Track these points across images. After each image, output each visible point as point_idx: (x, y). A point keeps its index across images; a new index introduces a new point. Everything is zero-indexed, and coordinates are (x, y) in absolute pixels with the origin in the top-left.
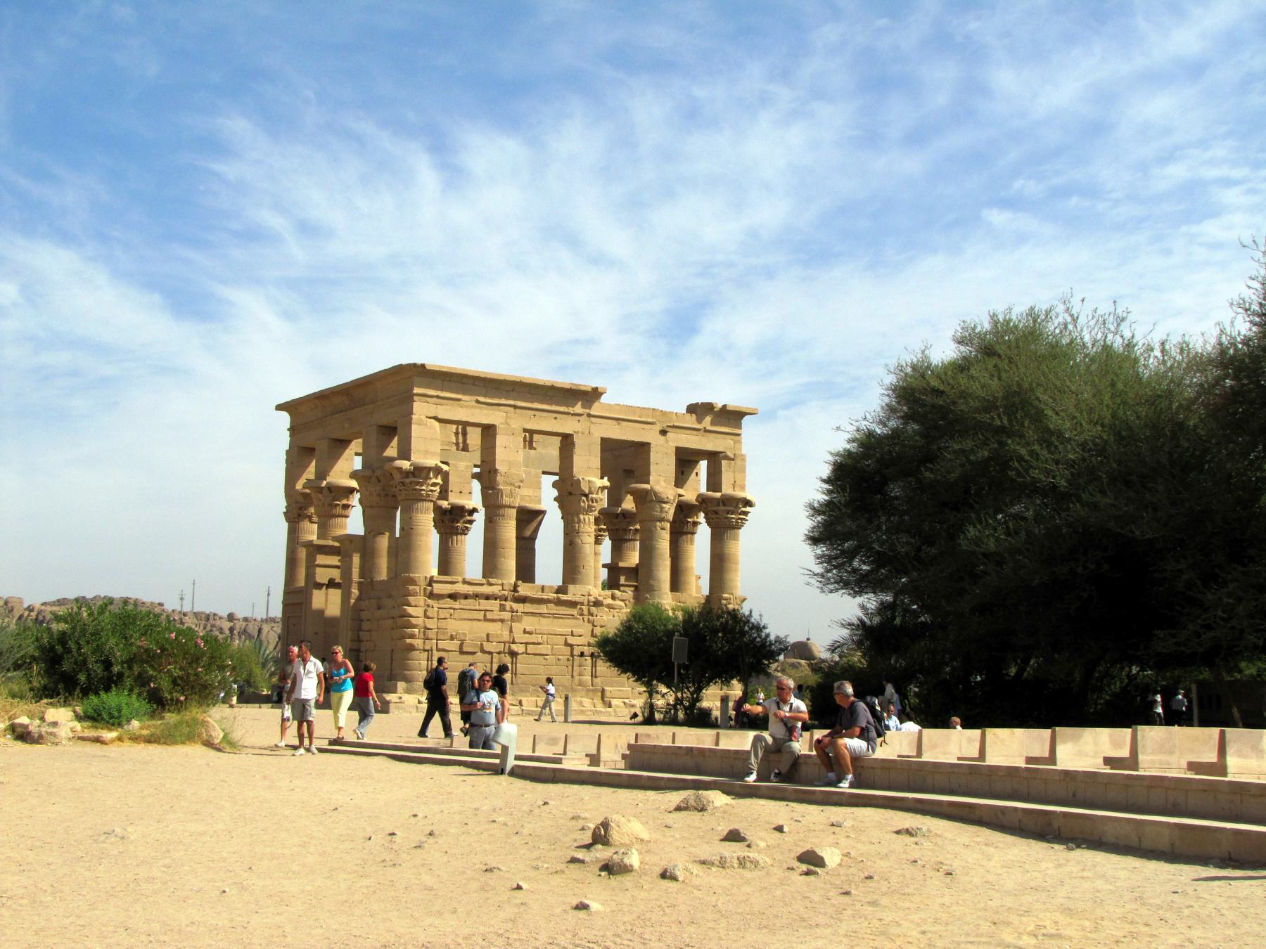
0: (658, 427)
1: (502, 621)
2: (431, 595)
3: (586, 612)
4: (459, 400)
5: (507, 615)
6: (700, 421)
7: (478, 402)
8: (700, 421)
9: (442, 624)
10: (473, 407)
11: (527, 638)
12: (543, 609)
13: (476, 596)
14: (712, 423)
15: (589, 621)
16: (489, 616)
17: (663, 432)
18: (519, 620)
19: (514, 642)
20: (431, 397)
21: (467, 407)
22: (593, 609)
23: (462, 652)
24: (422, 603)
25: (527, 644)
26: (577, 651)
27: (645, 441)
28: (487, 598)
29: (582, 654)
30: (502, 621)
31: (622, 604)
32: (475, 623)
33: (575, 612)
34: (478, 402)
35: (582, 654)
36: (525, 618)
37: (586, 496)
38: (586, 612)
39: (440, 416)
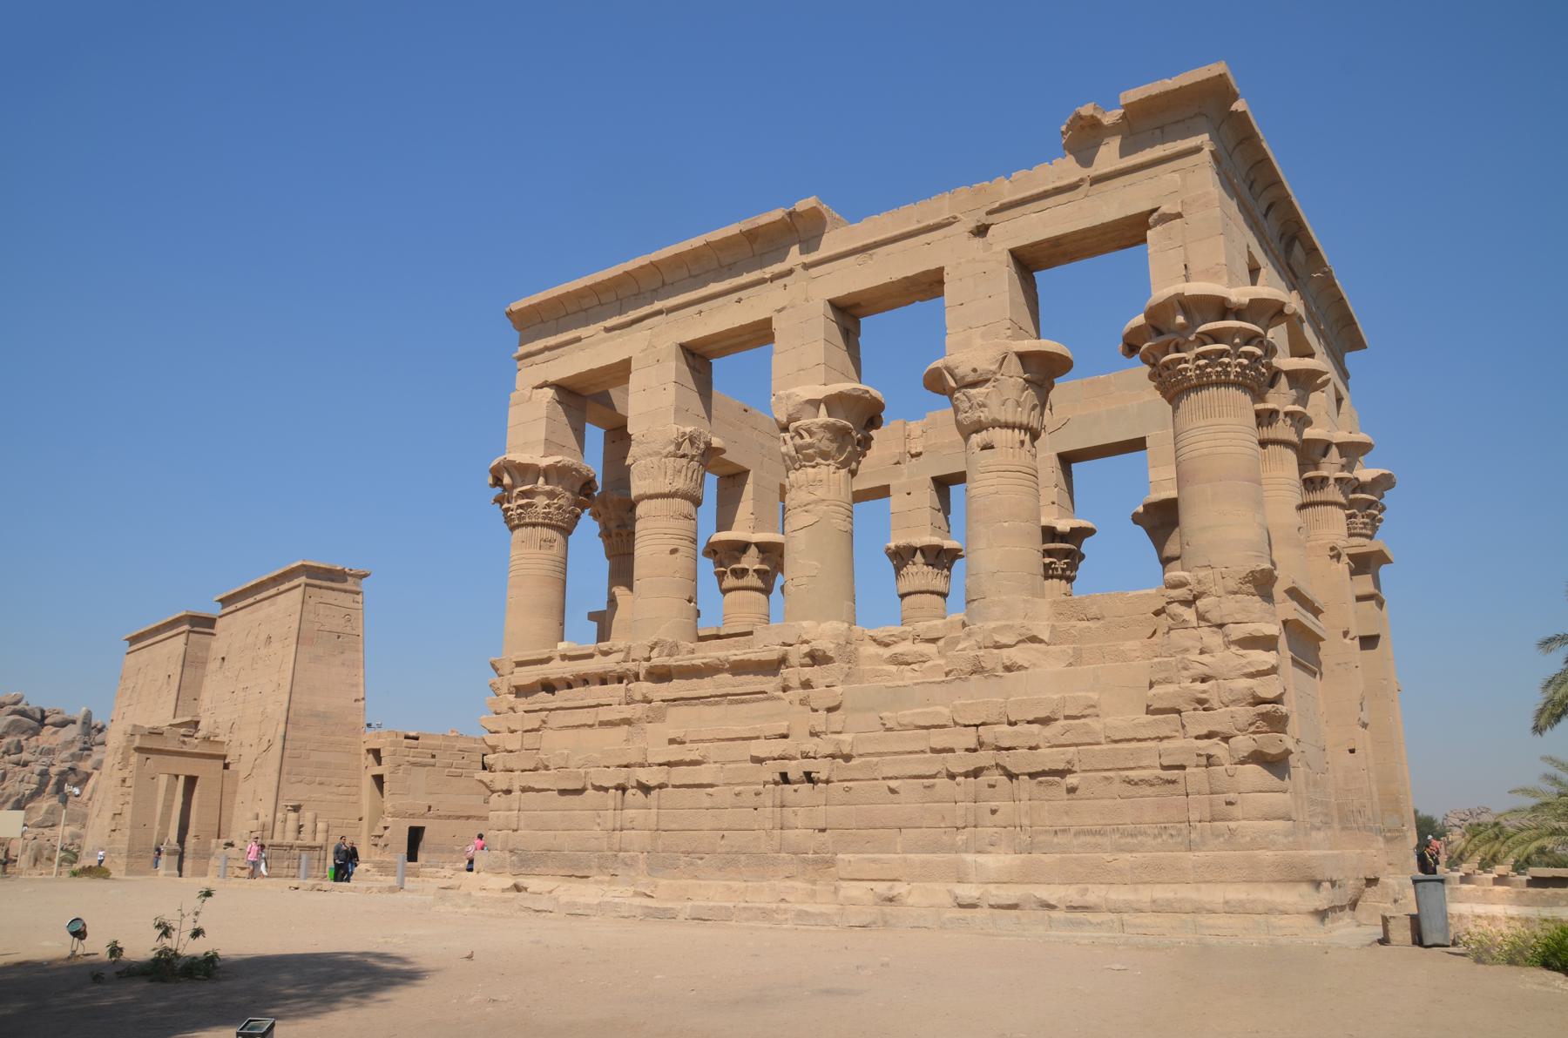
1: (627, 722)
3: (794, 682)
4: (579, 339)
5: (638, 710)
6: (1086, 162)
7: (608, 330)
8: (1086, 162)
10: (604, 340)
11: (675, 753)
12: (705, 686)
13: (585, 681)
14: (1124, 152)
15: (803, 702)
16: (605, 714)
17: (981, 231)
18: (656, 717)
20: (541, 351)
22: (808, 672)
23: (563, 792)
24: (504, 707)
25: (669, 764)
26: (770, 771)
27: (932, 265)
28: (604, 682)
29: (785, 779)
30: (627, 722)
31: (930, 649)
33: (770, 684)
34: (608, 330)
36: (676, 712)
38: (794, 682)
39: (552, 379)
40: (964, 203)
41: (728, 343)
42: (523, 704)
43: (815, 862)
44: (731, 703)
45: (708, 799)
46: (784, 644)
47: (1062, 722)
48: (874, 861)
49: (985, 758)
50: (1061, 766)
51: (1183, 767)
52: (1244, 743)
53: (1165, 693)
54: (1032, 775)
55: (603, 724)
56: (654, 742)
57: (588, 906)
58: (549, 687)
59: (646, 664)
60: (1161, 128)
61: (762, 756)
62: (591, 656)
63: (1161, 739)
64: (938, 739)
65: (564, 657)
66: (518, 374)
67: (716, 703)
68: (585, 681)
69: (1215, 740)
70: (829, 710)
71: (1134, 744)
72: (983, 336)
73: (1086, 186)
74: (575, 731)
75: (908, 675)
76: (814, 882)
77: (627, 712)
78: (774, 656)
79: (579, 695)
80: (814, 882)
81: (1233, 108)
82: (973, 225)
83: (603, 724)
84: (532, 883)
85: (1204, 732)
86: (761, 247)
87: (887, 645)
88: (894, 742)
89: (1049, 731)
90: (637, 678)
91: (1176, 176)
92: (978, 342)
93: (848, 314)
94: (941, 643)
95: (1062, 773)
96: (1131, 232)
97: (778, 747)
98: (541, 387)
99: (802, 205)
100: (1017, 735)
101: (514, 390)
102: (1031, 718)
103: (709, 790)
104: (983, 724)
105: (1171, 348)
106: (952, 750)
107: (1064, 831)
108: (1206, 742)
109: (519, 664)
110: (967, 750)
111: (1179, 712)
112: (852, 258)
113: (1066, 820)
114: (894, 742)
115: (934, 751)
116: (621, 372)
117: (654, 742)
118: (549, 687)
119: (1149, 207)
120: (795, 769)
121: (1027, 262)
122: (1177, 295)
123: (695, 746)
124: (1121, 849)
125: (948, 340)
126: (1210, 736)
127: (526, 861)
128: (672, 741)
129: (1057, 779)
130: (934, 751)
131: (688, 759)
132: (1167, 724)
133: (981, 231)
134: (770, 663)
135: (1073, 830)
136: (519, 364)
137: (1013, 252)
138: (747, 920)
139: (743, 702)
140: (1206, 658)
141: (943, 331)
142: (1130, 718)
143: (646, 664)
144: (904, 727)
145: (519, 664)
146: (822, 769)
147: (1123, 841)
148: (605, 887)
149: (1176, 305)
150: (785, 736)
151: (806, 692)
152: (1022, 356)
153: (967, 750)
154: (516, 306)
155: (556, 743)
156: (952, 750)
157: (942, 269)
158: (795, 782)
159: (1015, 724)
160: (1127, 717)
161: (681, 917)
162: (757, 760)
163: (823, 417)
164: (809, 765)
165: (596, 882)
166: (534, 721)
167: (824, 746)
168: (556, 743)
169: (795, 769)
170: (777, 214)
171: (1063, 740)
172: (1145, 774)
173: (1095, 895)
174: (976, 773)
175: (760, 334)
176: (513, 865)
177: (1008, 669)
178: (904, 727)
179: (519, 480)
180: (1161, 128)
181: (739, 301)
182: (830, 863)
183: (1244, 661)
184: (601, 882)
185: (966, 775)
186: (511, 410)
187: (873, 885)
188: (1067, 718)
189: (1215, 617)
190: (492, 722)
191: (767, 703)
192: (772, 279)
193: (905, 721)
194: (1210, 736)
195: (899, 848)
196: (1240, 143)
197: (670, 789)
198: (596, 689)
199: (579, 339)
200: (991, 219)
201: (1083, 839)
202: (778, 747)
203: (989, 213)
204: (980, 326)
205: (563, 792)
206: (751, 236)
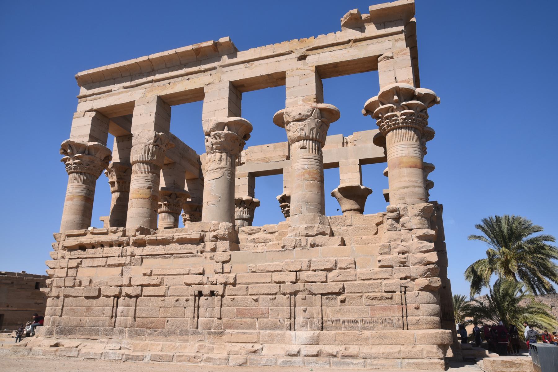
0: (294, 56)
2: (65, 248)
4: (111, 91)
9: (71, 272)
10: (122, 92)
13: (102, 245)
15: (212, 258)
16: (111, 261)
19: (130, 285)
21: (115, 94)
23: (87, 298)
24: (59, 256)
25: (142, 286)
27: (280, 70)
28: (111, 245)
29: (200, 294)
32: (98, 268)
35: (200, 294)
37: (209, 135)
40: (296, 46)
41: (181, 98)
42: (68, 254)
43: (215, 333)
44: (175, 257)
45: (162, 303)
46: (203, 231)
47: (338, 271)
48: (244, 333)
49: (300, 286)
50: (337, 291)
51: (394, 292)
52: (423, 282)
53: (387, 259)
54: (323, 295)
55: (110, 265)
56: (137, 274)
57: (96, 354)
58: (82, 247)
59: (134, 238)
60: (384, 23)
61: (189, 283)
62: (107, 233)
63: (385, 279)
64: (277, 277)
65: (93, 233)
66: (79, 105)
67: (167, 258)
68: (102, 245)
69: (409, 280)
70: (224, 262)
71: (372, 281)
72: (303, 100)
73: (351, 43)
74: (95, 268)
75: (260, 248)
76: (213, 343)
77: (122, 260)
78: (198, 236)
79: (98, 251)
80: (213, 343)
81: (411, 20)
82: (300, 55)
83: (110, 265)
84: (66, 342)
85: (404, 276)
86: (200, 57)
87: (250, 234)
88: (254, 278)
89: (331, 275)
90: (128, 245)
91: (391, 42)
92: (301, 103)
93: (237, 89)
94: (276, 234)
95: (338, 294)
96: (370, 65)
97: (199, 278)
98: (89, 111)
99: (224, 40)
100: (316, 276)
101: (76, 111)
102: (323, 268)
103: (163, 298)
104: (300, 271)
105: (390, 110)
106: (284, 282)
107: (337, 320)
108: (404, 281)
109: (69, 236)
110: (291, 282)
111: (393, 267)
112: (243, 65)
113: (339, 316)
114: (254, 278)
115: (275, 282)
116: (131, 105)
117: (137, 274)
118: (82, 247)
119: (379, 54)
120: (206, 289)
121: (323, 73)
122: (396, 87)
123: (156, 277)
124: (364, 328)
125: (287, 101)
126: (406, 278)
127: (65, 331)
128: (145, 275)
129: (335, 296)
130: (275, 282)
131: (152, 283)
132: (386, 273)
133: (302, 58)
134: (196, 239)
135: (342, 320)
136: (79, 100)
137: (317, 67)
138: (179, 361)
139: (181, 257)
140: (404, 243)
141: (285, 98)
142: (371, 268)
143: (134, 238)
144: (262, 271)
145: (69, 236)
146: (219, 289)
147: (366, 325)
148: (105, 345)
149: (395, 91)
150: (202, 274)
151: (213, 254)
152: (321, 110)
153: (291, 282)
154: (80, 74)
155: (84, 274)
156: (284, 282)
157: (285, 72)
158: (205, 296)
159: (315, 271)
160: (371, 268)
161: (146, 360)
162: (188, 285)
163: (226, 131)
164: (213, 288)
165: (101, 342)
166: (74, 263)
167: (221, 279)
168: (84, 274)
169: (206, 289)
170: (210, 43)
171: (338, 279)
172: (378, 295)
173: (353, 349)
174: (295, 293)
175: (198, 95)
176: (57, 333)
177: (313, 246)
178: (262, 271)
179: (75, 151)
180: (384, 23)
181: (189, 79)
182: (221, 334)
183: (422, 245)
184: (104, 342)
185: (291, 294)
186: (74, 120)
187: (244, 345)
188: (340, 268)
189: (408, 226)
190: (52, 264)
191: (193, 258)
192: (204, 71)
193: (262, 268)
194: (406, 278)
195: (257, 327)
196: (409, 37)
197: (142, 298)
198: (106, 248)
199: (111, 91)
200: (309, 53)
201: (346, 324)
202: (199, 278)
203: (307, 50)
204: (300, 97)
205: (87, 298)
206: (197, 51)
